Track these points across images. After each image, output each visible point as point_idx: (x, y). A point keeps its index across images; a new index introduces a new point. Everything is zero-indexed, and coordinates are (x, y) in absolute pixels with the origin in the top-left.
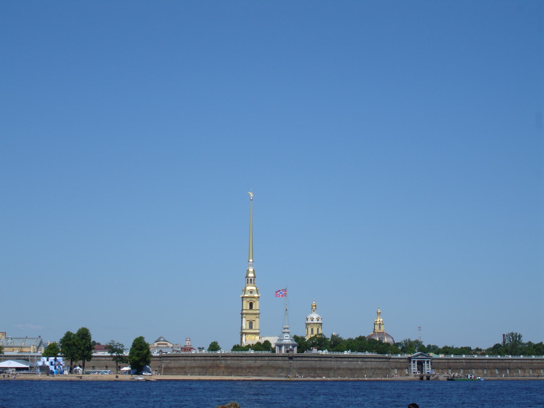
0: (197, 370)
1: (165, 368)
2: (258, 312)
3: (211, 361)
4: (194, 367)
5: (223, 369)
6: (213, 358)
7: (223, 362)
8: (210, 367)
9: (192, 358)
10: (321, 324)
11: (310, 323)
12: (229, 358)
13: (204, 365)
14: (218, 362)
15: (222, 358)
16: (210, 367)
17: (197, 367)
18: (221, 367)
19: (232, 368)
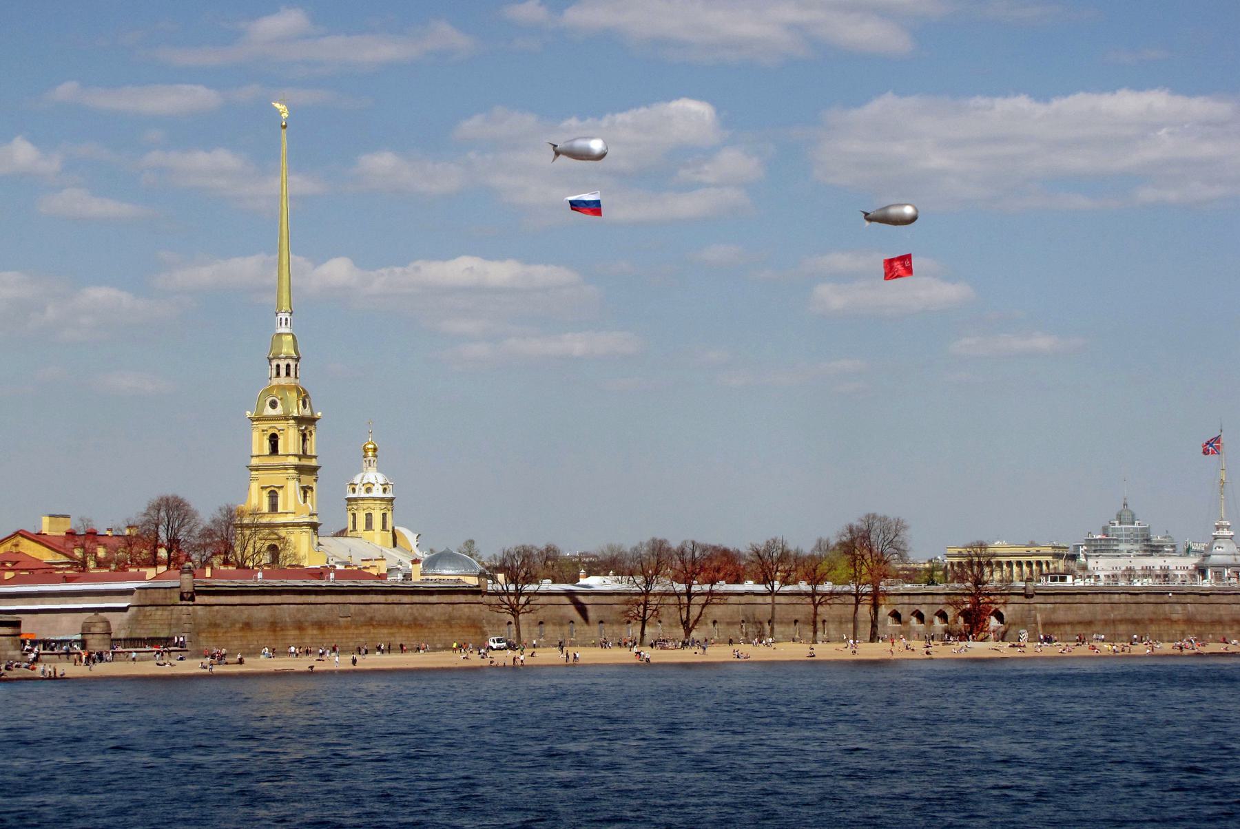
0: (1122, 628)
1: (1044, 625)
2: (314, 463)
3: (1151, 607)
4: (1114, 622)
5: (1183, 627)
6: (1153, 599)
7: (1178, 607)
8: (1152, 621)
9: (1106, 598)
10: (391, 500)
11: (382, 499)
12: (1189, 599)
13: (1136, 617)
14: (1167, 607)
15: (1174, 599)
16: (1152, 621)
17: (1121, 621)
18: (1176, 622)
19: (1201, 623)
